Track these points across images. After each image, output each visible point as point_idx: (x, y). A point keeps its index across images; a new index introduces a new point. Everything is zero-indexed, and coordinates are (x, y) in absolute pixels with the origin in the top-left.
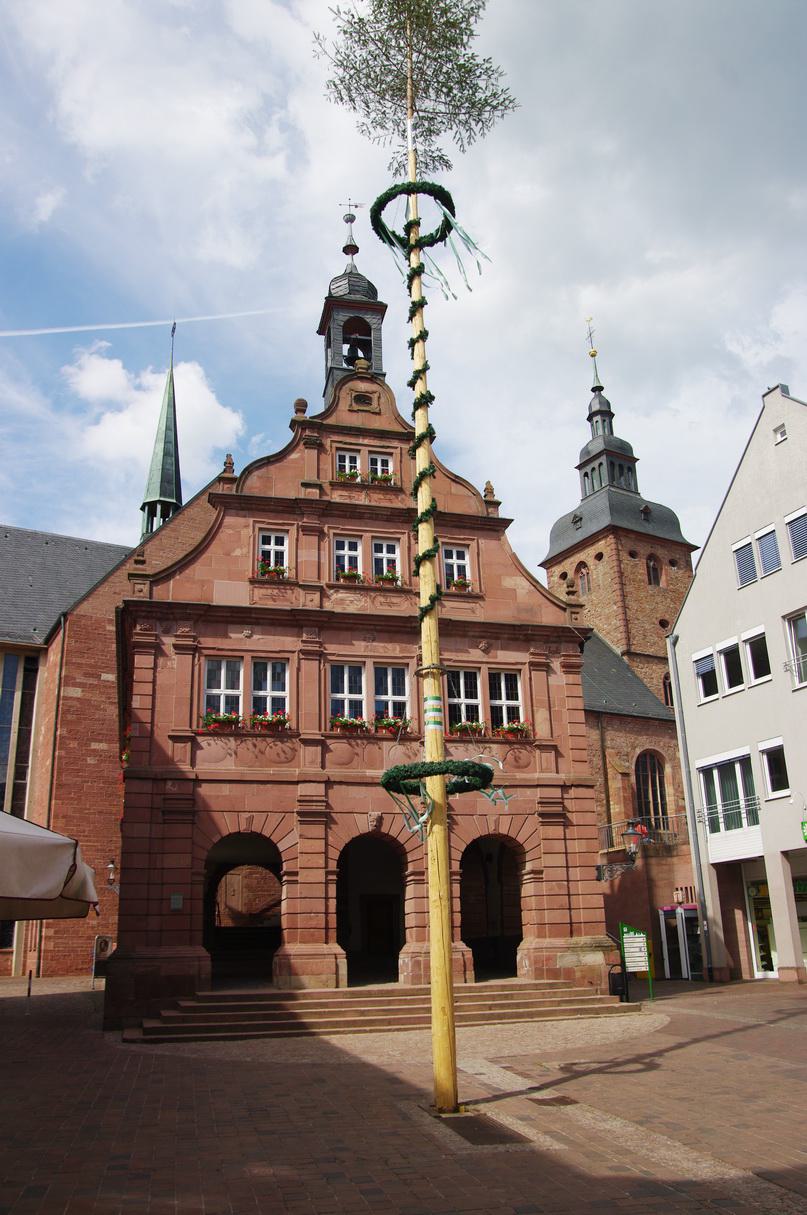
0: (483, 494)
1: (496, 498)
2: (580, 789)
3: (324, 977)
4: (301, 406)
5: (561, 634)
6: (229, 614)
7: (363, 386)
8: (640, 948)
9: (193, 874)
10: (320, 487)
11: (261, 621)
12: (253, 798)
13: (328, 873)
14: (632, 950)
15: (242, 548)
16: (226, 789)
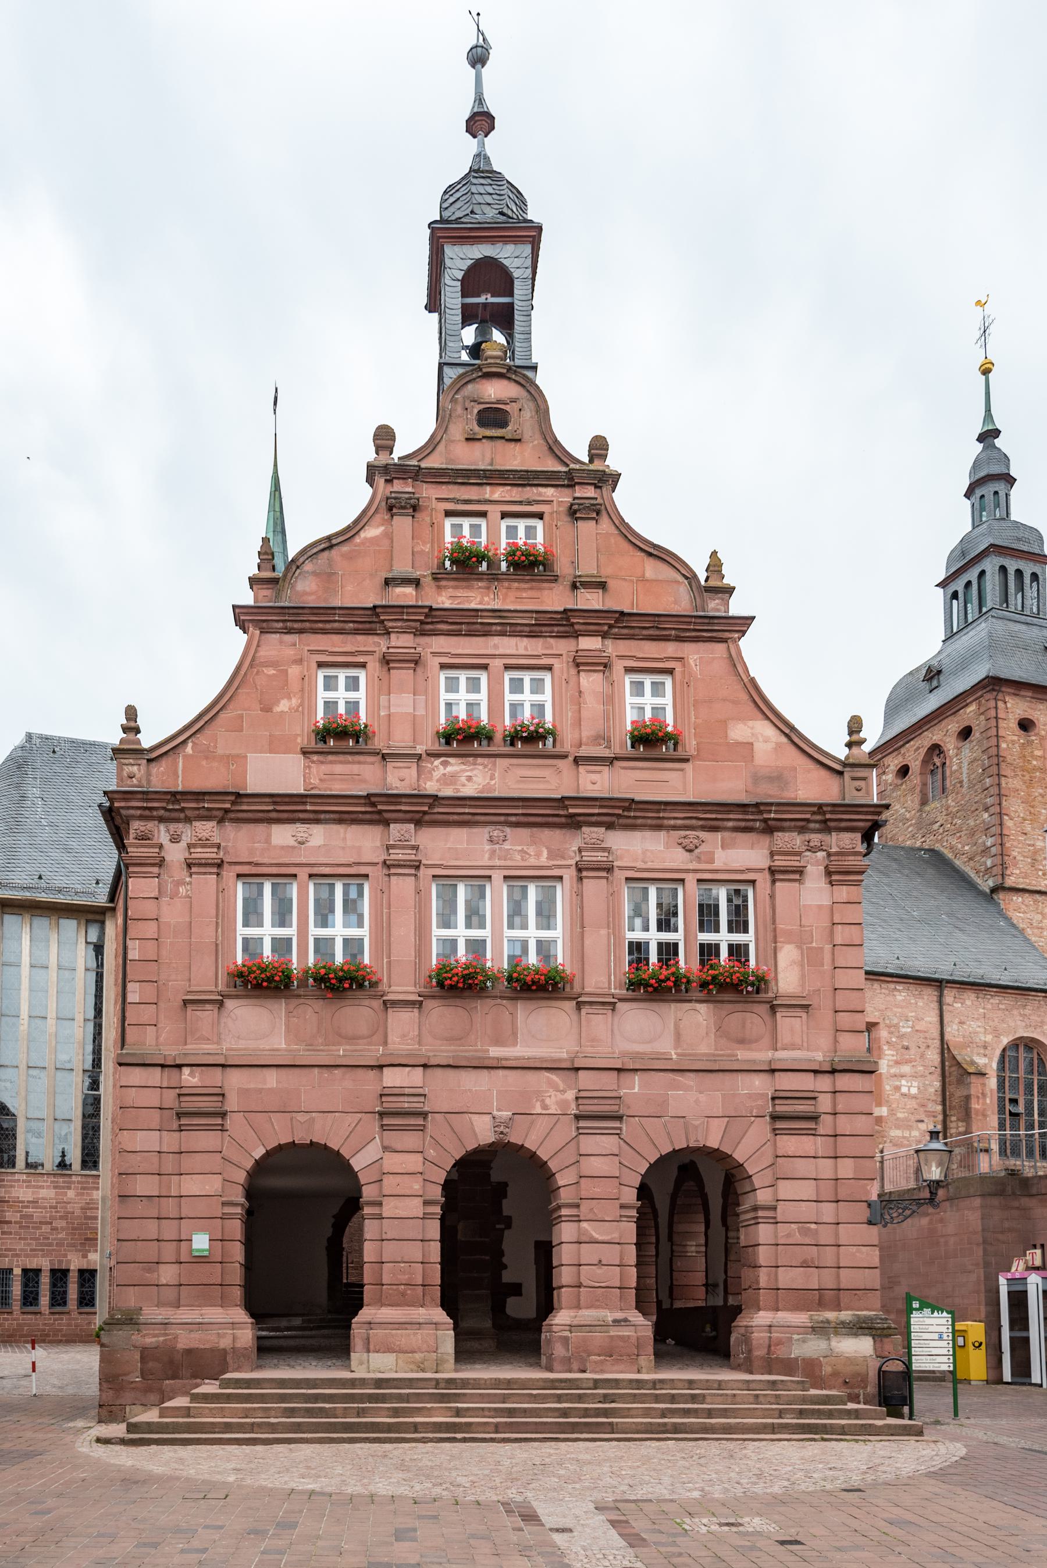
0: (702, 576)
1: (725, 581)
2: (847, 1077)
3: (418, 1356)
4: (384, 437)
5: (828, 816)
6: (271, 808)
7: (494, 391)
8: (941, 1334)
9: (224, 1204)
10: (416, 583)
11: (322, 816)
12: (310, 1090)
13: (426, 1203)
14: (925, 1336)
15: (289, 698)
16: (271, 1079)
